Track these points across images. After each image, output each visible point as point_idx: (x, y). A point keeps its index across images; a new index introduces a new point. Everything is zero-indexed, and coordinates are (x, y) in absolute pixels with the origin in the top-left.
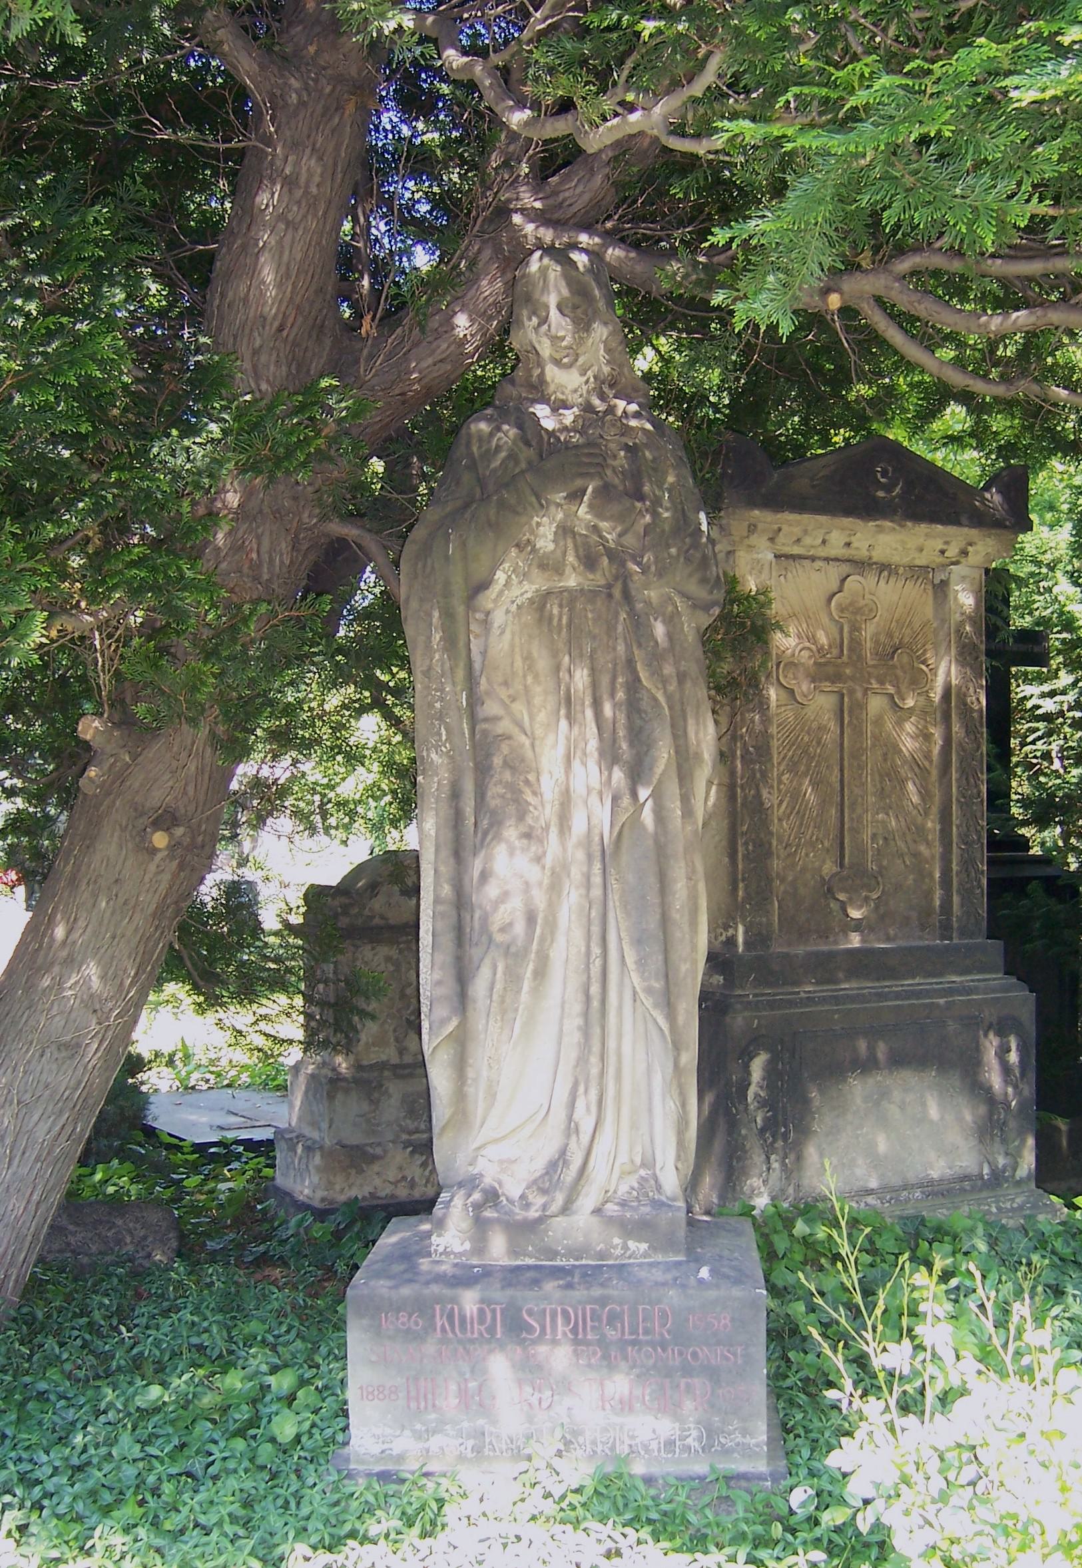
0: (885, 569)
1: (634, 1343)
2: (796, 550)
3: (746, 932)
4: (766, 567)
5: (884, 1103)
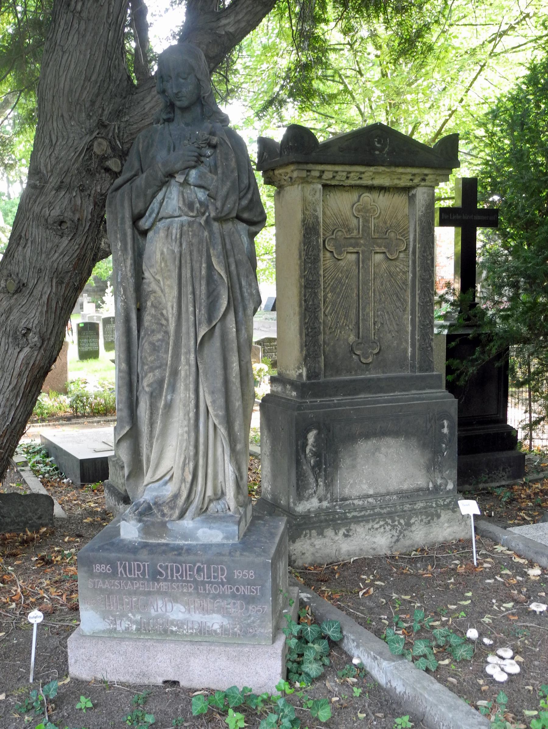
0: (382, 189)
1: (209, 583)
2: (333, 183)
4: (318, 191)
5: (377, 454)
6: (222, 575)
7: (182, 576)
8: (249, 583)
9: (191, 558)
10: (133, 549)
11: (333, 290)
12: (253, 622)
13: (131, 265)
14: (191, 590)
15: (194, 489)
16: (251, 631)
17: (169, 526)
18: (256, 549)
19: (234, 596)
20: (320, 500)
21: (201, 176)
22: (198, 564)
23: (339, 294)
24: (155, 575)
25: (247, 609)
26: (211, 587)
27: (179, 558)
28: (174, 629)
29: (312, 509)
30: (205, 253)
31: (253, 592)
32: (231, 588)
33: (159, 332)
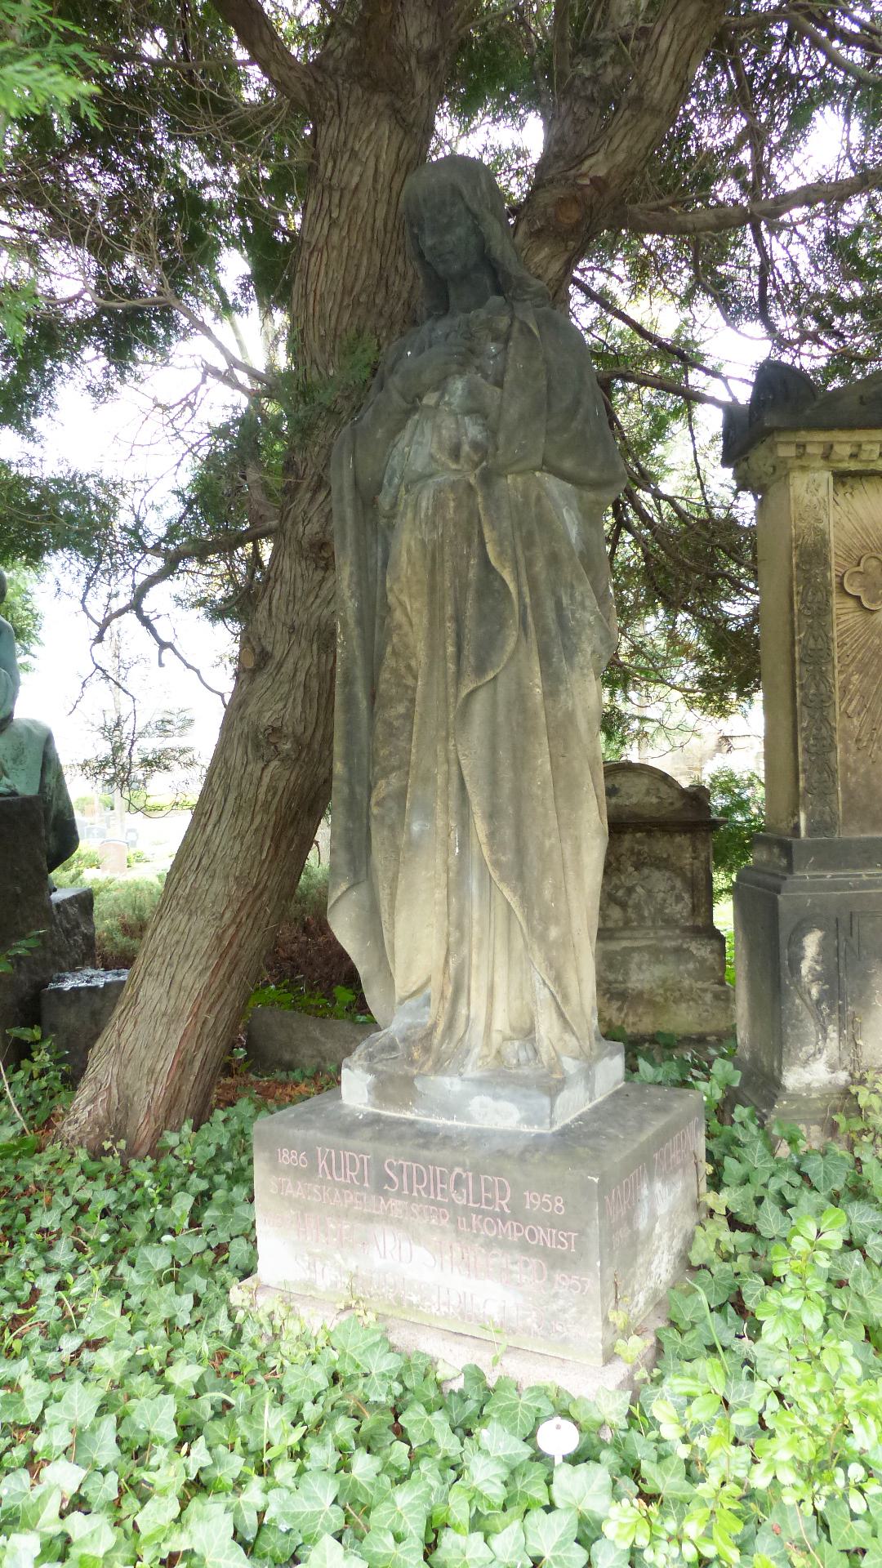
1: (479, 1212)
2: (853, 466)
3: (808, 819)
4: (824, 485)
6: (503, 1198)
7: (427, 1190)
8: (552, 1222)
9: (445, 1154)
10: (350, 1127)
11: (863, 669)
12: (564, 1310)
13: (351, 574)
14: (444, 1222)
15: (463, 1011)
16: (559, 1328)
17: (418, 1084)
18: (580, 1150)
19: (524, 1247)
20: (833, 1068)
21: (472, 392)
22: (458, 1170)
23: (875, 677)
24: (382, 1183)
25: (550, 1279)
26: (482, 1221)
27: (425, 1153)
28: (415, 1299)
29: (815, 1085)
30: (476, 540)
31: (563, 1245)
32: (519, 1230)
33: (400, 701)
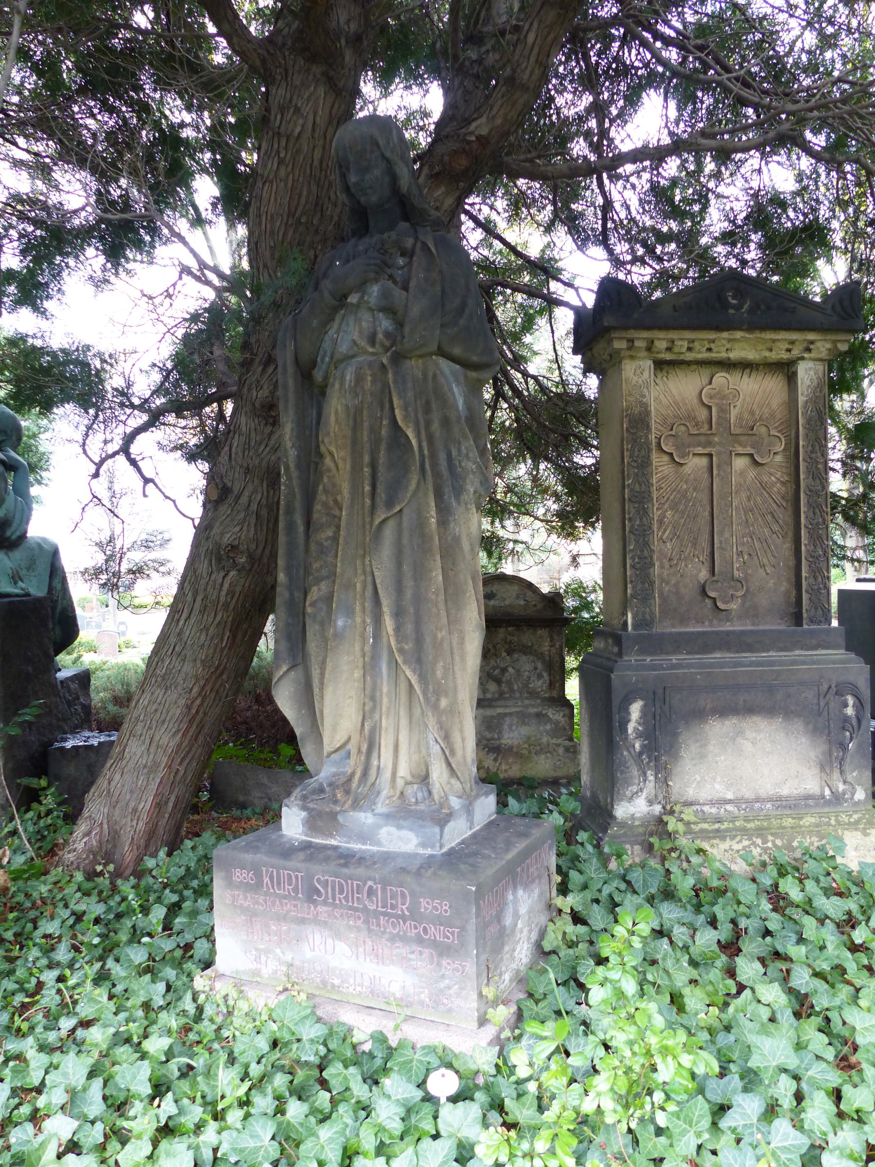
0: (745, 366)
1: (385, 914)
2: (668, 356)
3: (633, 618)
5: (739, 740)
8: (440, 921)
9: (361, 871)
10: (288, 851)
11: (674, 507)
12: (449, 988)
14: (359, 923)
17: (340, 818)
18: (462, 867)
19: (420, 940)
20: (650, 802)
21: (385, 294)
22: (370, 883)
23: (683, 512)
24: (312, 894)
25: (439, 964)
27: (346, 871)
28: (336, 982)
29: (638, 815)
30: (387, 406)
